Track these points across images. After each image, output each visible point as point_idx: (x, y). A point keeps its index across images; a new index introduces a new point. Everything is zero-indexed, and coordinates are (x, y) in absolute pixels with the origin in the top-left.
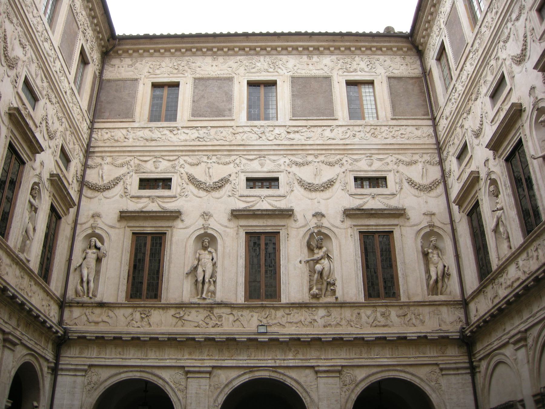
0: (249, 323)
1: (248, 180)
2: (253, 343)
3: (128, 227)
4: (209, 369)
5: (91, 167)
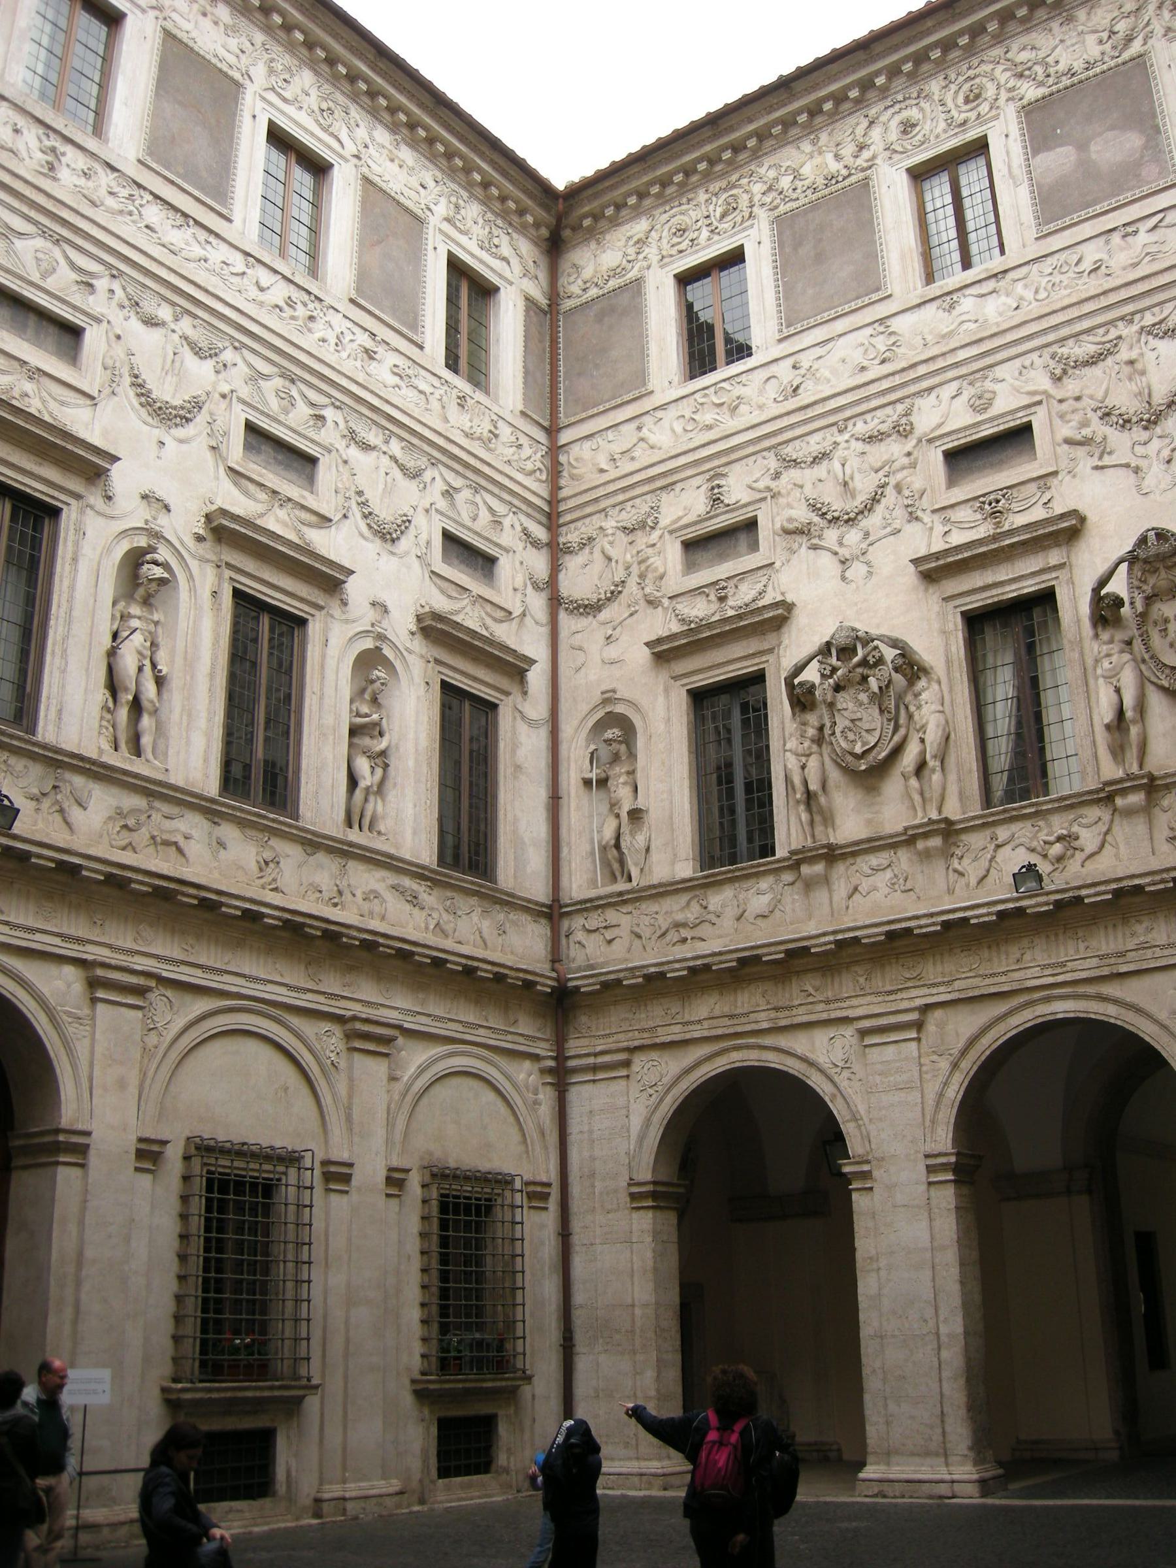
2: (1008, 926)
4: (914, 1016)
5: (569, 551)
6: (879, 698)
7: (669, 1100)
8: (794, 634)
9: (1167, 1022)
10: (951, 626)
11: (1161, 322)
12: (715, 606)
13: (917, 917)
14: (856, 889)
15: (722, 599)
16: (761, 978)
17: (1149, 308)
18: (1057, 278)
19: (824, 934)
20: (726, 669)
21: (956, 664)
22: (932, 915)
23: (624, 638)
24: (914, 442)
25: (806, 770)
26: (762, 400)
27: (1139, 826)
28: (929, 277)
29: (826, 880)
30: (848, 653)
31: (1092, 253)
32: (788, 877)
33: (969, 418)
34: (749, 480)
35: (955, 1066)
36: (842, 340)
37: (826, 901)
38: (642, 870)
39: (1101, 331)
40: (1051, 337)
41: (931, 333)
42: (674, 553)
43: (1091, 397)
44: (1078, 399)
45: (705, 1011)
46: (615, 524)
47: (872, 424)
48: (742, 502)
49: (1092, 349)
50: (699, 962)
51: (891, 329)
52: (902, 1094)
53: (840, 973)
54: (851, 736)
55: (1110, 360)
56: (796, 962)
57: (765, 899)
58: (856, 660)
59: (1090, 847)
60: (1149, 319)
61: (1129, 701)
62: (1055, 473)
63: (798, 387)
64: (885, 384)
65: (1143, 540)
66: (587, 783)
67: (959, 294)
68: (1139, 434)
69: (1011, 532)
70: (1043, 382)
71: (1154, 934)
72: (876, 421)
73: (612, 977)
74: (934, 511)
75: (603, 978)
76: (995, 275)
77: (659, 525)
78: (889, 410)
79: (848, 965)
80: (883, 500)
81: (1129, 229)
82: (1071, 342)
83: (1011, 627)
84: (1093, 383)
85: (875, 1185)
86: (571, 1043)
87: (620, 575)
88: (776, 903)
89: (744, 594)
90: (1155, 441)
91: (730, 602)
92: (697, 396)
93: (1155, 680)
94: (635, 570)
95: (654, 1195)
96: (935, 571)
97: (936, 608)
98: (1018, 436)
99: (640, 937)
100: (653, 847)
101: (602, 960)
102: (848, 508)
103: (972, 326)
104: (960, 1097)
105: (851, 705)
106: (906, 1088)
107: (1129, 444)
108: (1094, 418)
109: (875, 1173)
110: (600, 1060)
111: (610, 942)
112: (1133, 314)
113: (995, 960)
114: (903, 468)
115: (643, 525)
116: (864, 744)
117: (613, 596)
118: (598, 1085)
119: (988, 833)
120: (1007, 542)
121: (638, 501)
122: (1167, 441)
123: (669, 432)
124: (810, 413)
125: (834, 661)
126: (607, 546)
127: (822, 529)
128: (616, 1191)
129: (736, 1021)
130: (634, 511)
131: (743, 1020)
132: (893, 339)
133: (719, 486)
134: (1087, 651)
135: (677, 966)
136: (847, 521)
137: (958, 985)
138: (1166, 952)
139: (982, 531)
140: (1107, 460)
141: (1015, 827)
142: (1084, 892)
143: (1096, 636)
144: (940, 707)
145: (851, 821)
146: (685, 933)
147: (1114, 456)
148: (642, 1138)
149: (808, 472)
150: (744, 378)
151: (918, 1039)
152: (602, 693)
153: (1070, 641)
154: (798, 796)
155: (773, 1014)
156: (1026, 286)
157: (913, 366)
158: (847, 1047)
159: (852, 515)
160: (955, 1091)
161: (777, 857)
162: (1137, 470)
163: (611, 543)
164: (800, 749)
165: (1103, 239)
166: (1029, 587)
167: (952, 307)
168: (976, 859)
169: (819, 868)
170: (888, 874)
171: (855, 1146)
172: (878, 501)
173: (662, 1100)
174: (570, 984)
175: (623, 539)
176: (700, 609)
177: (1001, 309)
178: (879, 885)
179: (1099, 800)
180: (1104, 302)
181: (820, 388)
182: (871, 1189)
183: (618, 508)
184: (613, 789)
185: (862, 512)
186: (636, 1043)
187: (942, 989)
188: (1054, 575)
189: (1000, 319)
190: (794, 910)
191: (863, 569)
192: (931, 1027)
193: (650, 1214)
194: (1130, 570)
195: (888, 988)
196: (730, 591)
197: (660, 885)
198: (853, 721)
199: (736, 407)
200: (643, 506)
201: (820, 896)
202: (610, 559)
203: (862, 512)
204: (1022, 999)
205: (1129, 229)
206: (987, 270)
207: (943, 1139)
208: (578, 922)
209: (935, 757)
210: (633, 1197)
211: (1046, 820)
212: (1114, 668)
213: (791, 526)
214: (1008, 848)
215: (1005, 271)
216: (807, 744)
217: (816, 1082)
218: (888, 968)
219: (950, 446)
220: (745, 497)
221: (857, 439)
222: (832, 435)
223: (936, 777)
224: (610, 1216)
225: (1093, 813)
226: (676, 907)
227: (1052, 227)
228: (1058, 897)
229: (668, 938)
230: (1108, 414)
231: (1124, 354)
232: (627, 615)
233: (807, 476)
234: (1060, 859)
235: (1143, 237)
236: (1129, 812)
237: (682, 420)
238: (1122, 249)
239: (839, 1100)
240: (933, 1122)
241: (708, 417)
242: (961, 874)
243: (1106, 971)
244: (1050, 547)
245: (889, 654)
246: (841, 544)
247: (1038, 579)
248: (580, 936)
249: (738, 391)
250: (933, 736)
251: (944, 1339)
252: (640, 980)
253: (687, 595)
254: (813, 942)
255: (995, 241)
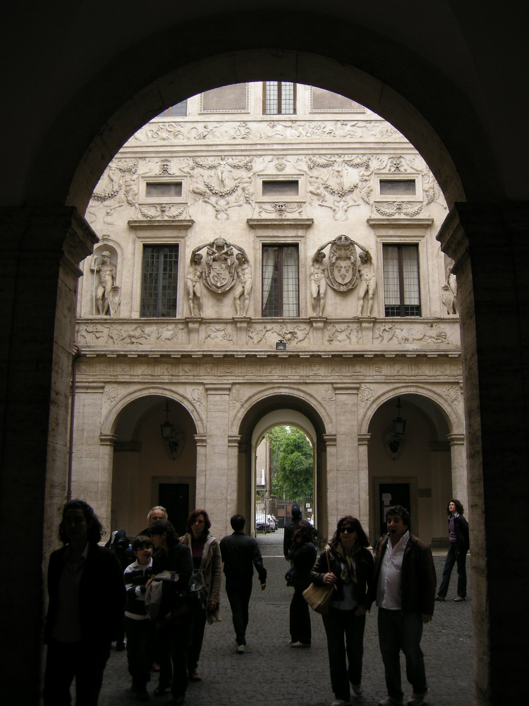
0: (266, 339)
1: (266, 184)
2: (272, 360)
3: (139, 238)
4: (229, 386)
6: (229, 267)
7: (120, 404)
8: (193, 233)
9: (321, 401)
10: (257, 247)
11: (350, 161)
12: (159, 213)
13: (237, 351)
14: (209, 336)
15: (163, 211)
16: (167, 363)
17: (347, 154)
18: (315, 131)
19: (199, 351)
20: (162, 240)
21: (258, 262)
22: (243, 352)
23: (115, 215)
24: (252, 174)
25: (195, 288)
26: (189, 136)
27: (319, 334)
28: (264, 112)
29: (197, 331)
30: (220, 249)
31: (330, 126)
32: (181, 326)
33: (275, 172)
34: (181, 167)
35: (242, 406)
36: (226, 123)
37: (197, 338)
38: (115, 312)
39: (329, 156)
40: (310, 152)
41: (264, 133)
42: (143, 187)
43: (322, 179)
44: (317, 178)
45: (141, 372)
46: (116, 166)
47: (235, 161)
48: (176, 175)
49: (325, 162)
50: (143, 353)
51: (247, 127)
52: (221, 414)
53: (200, 366)
54: (216, 279)
55: (330, 168)
56: (186, 359)
57: (170, 333)
58: (224, 251)
59: (300, 338)
60: (347, 158)
61: (322, 291)
62: (305, 203)
63: (205, 136)
64: (243, 148)
65: (340, 238)
66: (92, 271)
67: (277, 122)
68: (336, 198)
69: (288, 220)
70: (306, 169)
71: (320, 371)
72: (237, 160)
73: (103, 353)
74: (256, 202)
75: (98, 353)
76: (292, 121)
77: (137, 173)
78: (243, 158)
79: (204, 364)
80: (236, 192)
81: (345, 123)
82: (317, 156)
83: (280, 252)
84: (324, 174)
85: (207, 445)
86: (77, 376)
87: (116, 188)
88: (174, 336)
89: (173, 212)
90: (342, 202)
91: (166, 213)
92: (160, 124)
93: (332, 286)
94: (123, 188)
95: (111, 440)
96: (254, 225)
97: (253, 239)
98: (292, 185)
99: (112, 338)
100: (121, 303)
101: (93, 344)
102: (221, 190)
103: (281, 137)
104: (243, 417)
105: (218, 268)
106: (224, 411)
107: (333, 200)
108: (322, 188)
109: (208, 441)
110: (91, 385)
111: (98, 338)
112: (341, 154)
113: (262, 371)
114: (247, 183)
115: (129, 170)
116: (221, 283)
117: (112, 196)
118: (88, 394)
119: (263, 325)
120: (285, 223)
121: (128, 160)
122: (346, 203)
123: (145, 135)
124: (210, 148)
125: (214, 250)
126: (111, 175)
127: (210, 196)
128: (93, 437)
129: (154, 378)
130: (125, 163)
131: (157, 378)
132: (248, 131)
133: (167, 165)
134: (308, 269)
135: (133, 353)
136: (220, 196)
137: (246, 377)
138: (323, 378)
139: (274, 216)
140: (324, 204)
141: (274, 325)
142: (300, 354)
143: (313, 265)
144: (254, 277)
145: (209, 310)
146: (133, 340)
147: (327, 203)
148: (107, 417)
149: (206, 171)
150: (182, 124)
151: (229, 395)
152: (103, 236)
153: (302, 264)
154: (191, 297)
155: (170, 377)
156: (303, 129)
157: (256, 144)
158: (200, 394)
159: (223, 194)
160: (241, 415)
161: (177, 318)
162: (334, 210)
163: (113, 174)
164: (194, 280)
165: (334, 122)
166: (289, 241)
167: (273, 127)
168: (257, 334)
169: (196, 326)
170: (223, 333)
171: (200, 429)
172: (234, 192)
173: (117, 404)
174: (82, 353)
175: (120, 174)
176: (152, 212)
177: (293, 134)
178: (219, 336)
179: (306, 322)
180: (332, 146)
181: (215, 139)
182: (206, 446)
183: (118, 160)
184: (103, 276)
185: (227, 194)
186: (108, 380)
187: (240, 378)
188: (299, 239)
189: (291, 138)
190: (182, 339)
191: (225, 216)
192: (234, 391)
193: (108, 447)
194: (332, 247)
195: (219, 374)
196: (167, 209)
197: (125, 319)
198: (218, 274)
199: (177, 135)
200: (130, 163)
201: (194, 336)
202: (112, 181)
203: (227, 194)
204: (270, 386)
205: (344, 123)
206: (289, 118)
207: (235, 431)
208: (83, 327)
209: (248, 294)
210: (101, 440)
211: (286, 325)
212: (319, 278)
213: (197, 191)
214: (270, 333)
215: (296, 121)
216: (196, 278)
217: (186, 404)
218: (219, 367)
219: (266, 179)
220: (178, 173)
221: (229, 165)
222: (218, 161)
223: (247, 302)
224: (90, 447)
225: (303, 326)
226: (130, 329)
227: (317, 111)
228: (291, 353)
229: (125, 341)
230: (327, 187)
231: (336, 167)
232: (118, 206)
233: (206, 173)
234: (289, 340)
235: (348, 128)
236: (317, 329)
237: (151, 132)
238: (340, 129)
239: (195, 413)
240: (232, 424)
241: (164, 135)
242: (252, 338)
243: (302, 381)
244: (299, 228)
245: (236, 252)
246: (217, 204)
247: (293, 239)
248: (84, 333)
249: (179, 128)
250: (248, 286)
251: (229, 500)
252: (116, 356)
253: (150, 206)
254: (194, 353)
255: (292, 107)
